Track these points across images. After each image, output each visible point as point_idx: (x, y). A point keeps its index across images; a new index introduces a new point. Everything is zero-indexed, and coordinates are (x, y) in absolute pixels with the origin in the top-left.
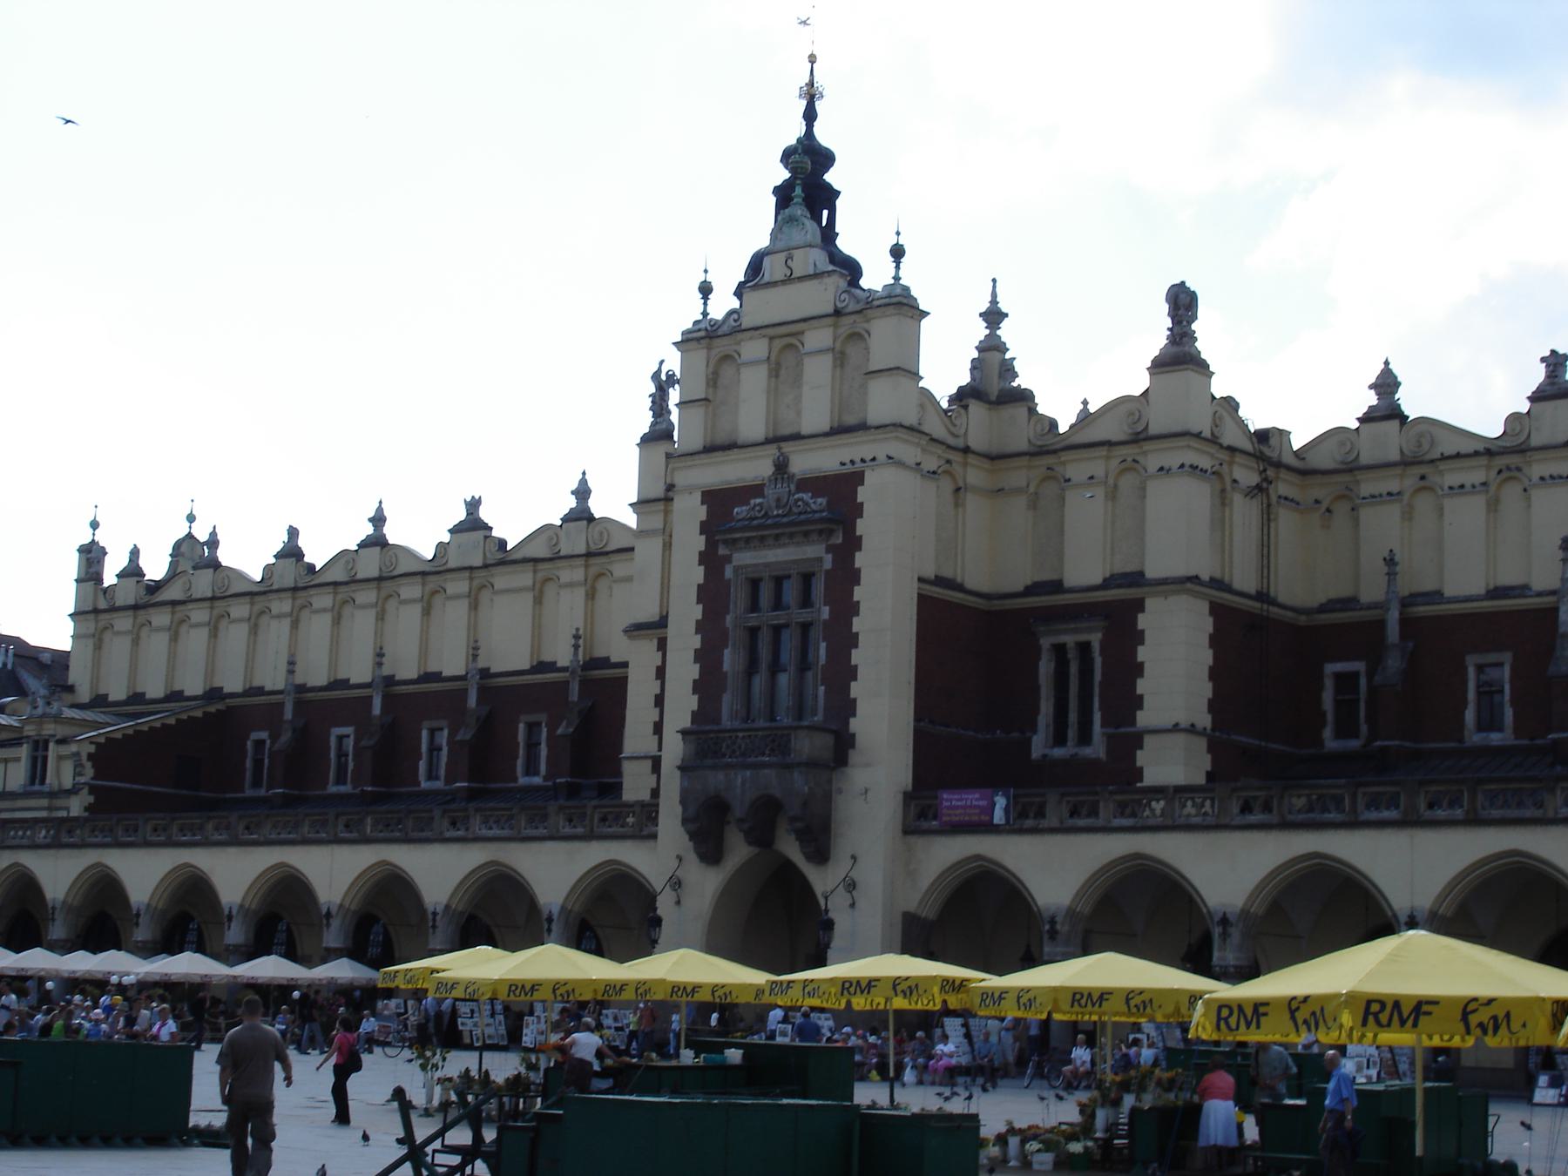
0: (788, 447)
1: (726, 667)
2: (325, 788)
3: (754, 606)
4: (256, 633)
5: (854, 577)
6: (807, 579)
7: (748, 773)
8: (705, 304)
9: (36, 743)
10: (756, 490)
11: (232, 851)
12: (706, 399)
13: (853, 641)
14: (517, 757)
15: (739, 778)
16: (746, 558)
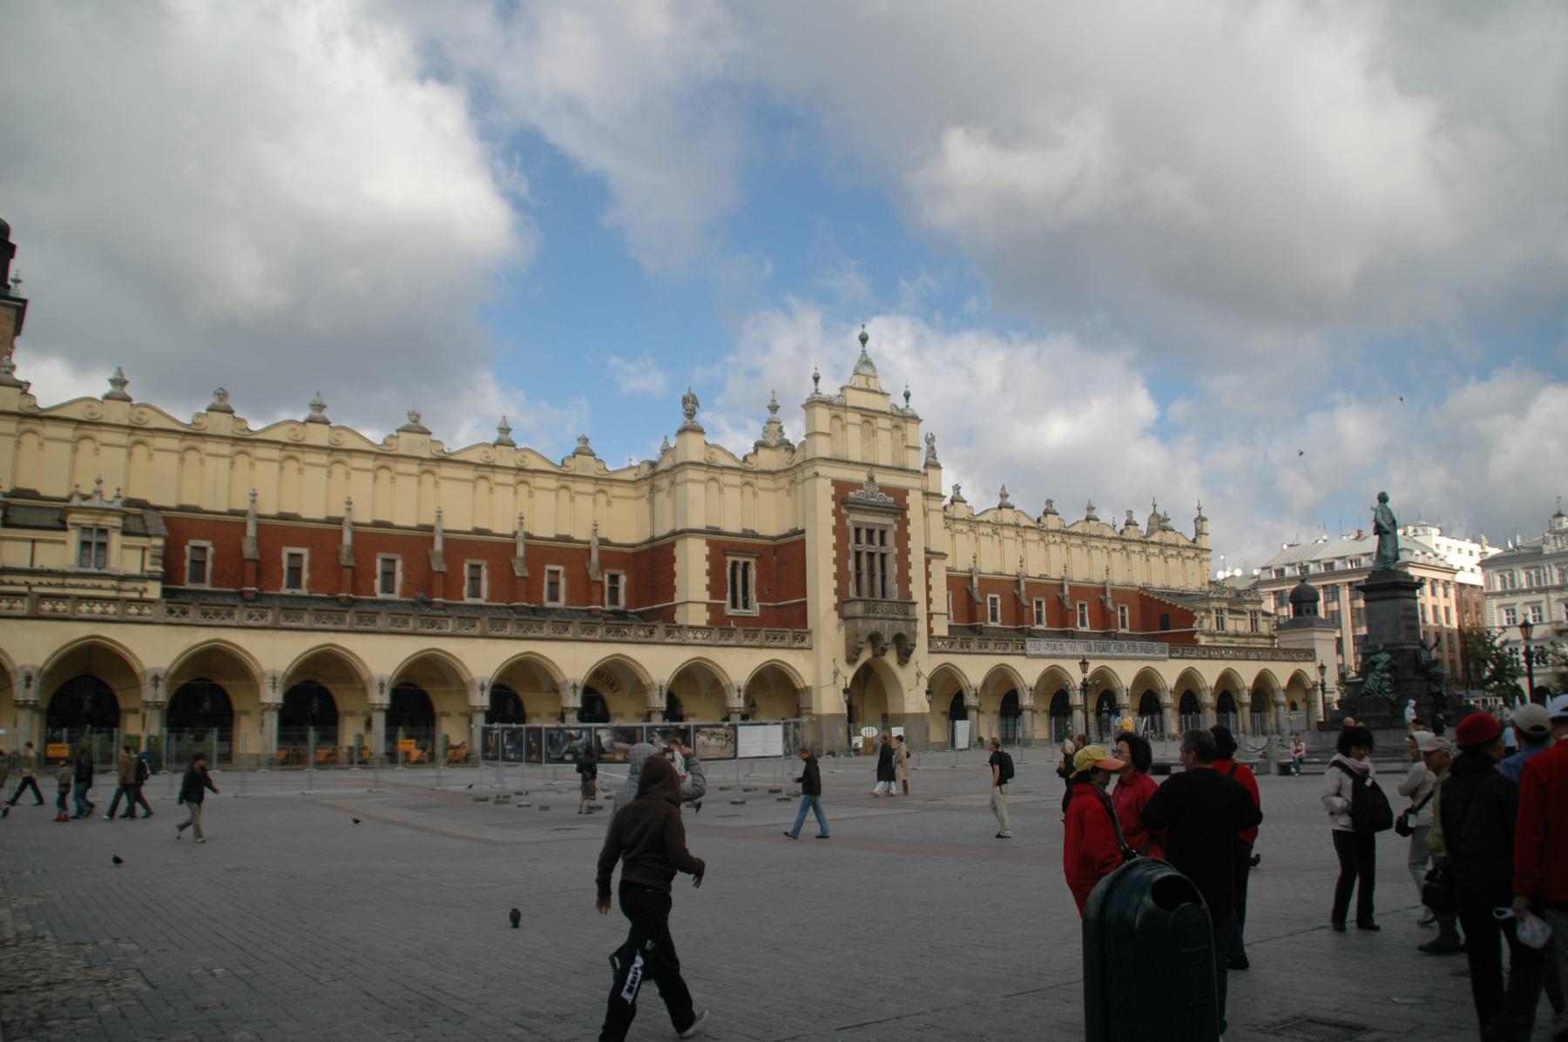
0: (875, 470)
1: (849, 569)
2: (278, 590)
3: (858, 541)
4: (182, 465)
5: (908, 537)
6: (882, 533)
7: (891, 622)
8: (816, 384)
9: (85, 529)
10: (859, 486)
11: (482, 642)
12: (828, 435)
13: (909, 566)
14: (463, 585)
15: (887, 624)
16: (855, 518)
